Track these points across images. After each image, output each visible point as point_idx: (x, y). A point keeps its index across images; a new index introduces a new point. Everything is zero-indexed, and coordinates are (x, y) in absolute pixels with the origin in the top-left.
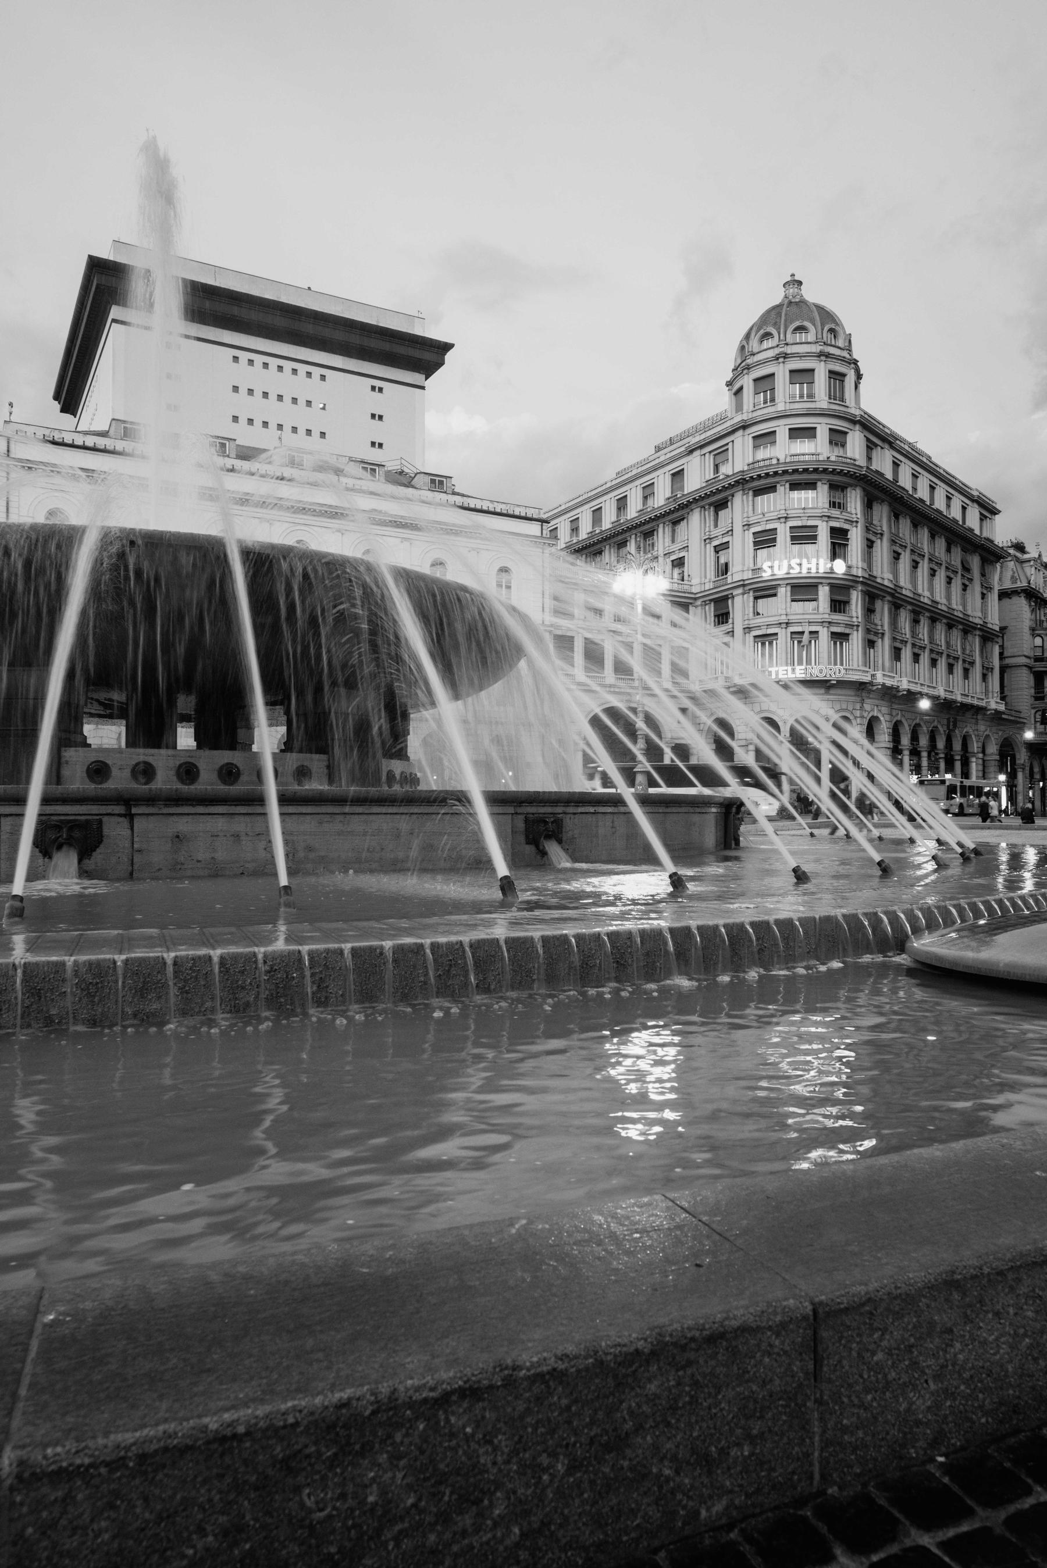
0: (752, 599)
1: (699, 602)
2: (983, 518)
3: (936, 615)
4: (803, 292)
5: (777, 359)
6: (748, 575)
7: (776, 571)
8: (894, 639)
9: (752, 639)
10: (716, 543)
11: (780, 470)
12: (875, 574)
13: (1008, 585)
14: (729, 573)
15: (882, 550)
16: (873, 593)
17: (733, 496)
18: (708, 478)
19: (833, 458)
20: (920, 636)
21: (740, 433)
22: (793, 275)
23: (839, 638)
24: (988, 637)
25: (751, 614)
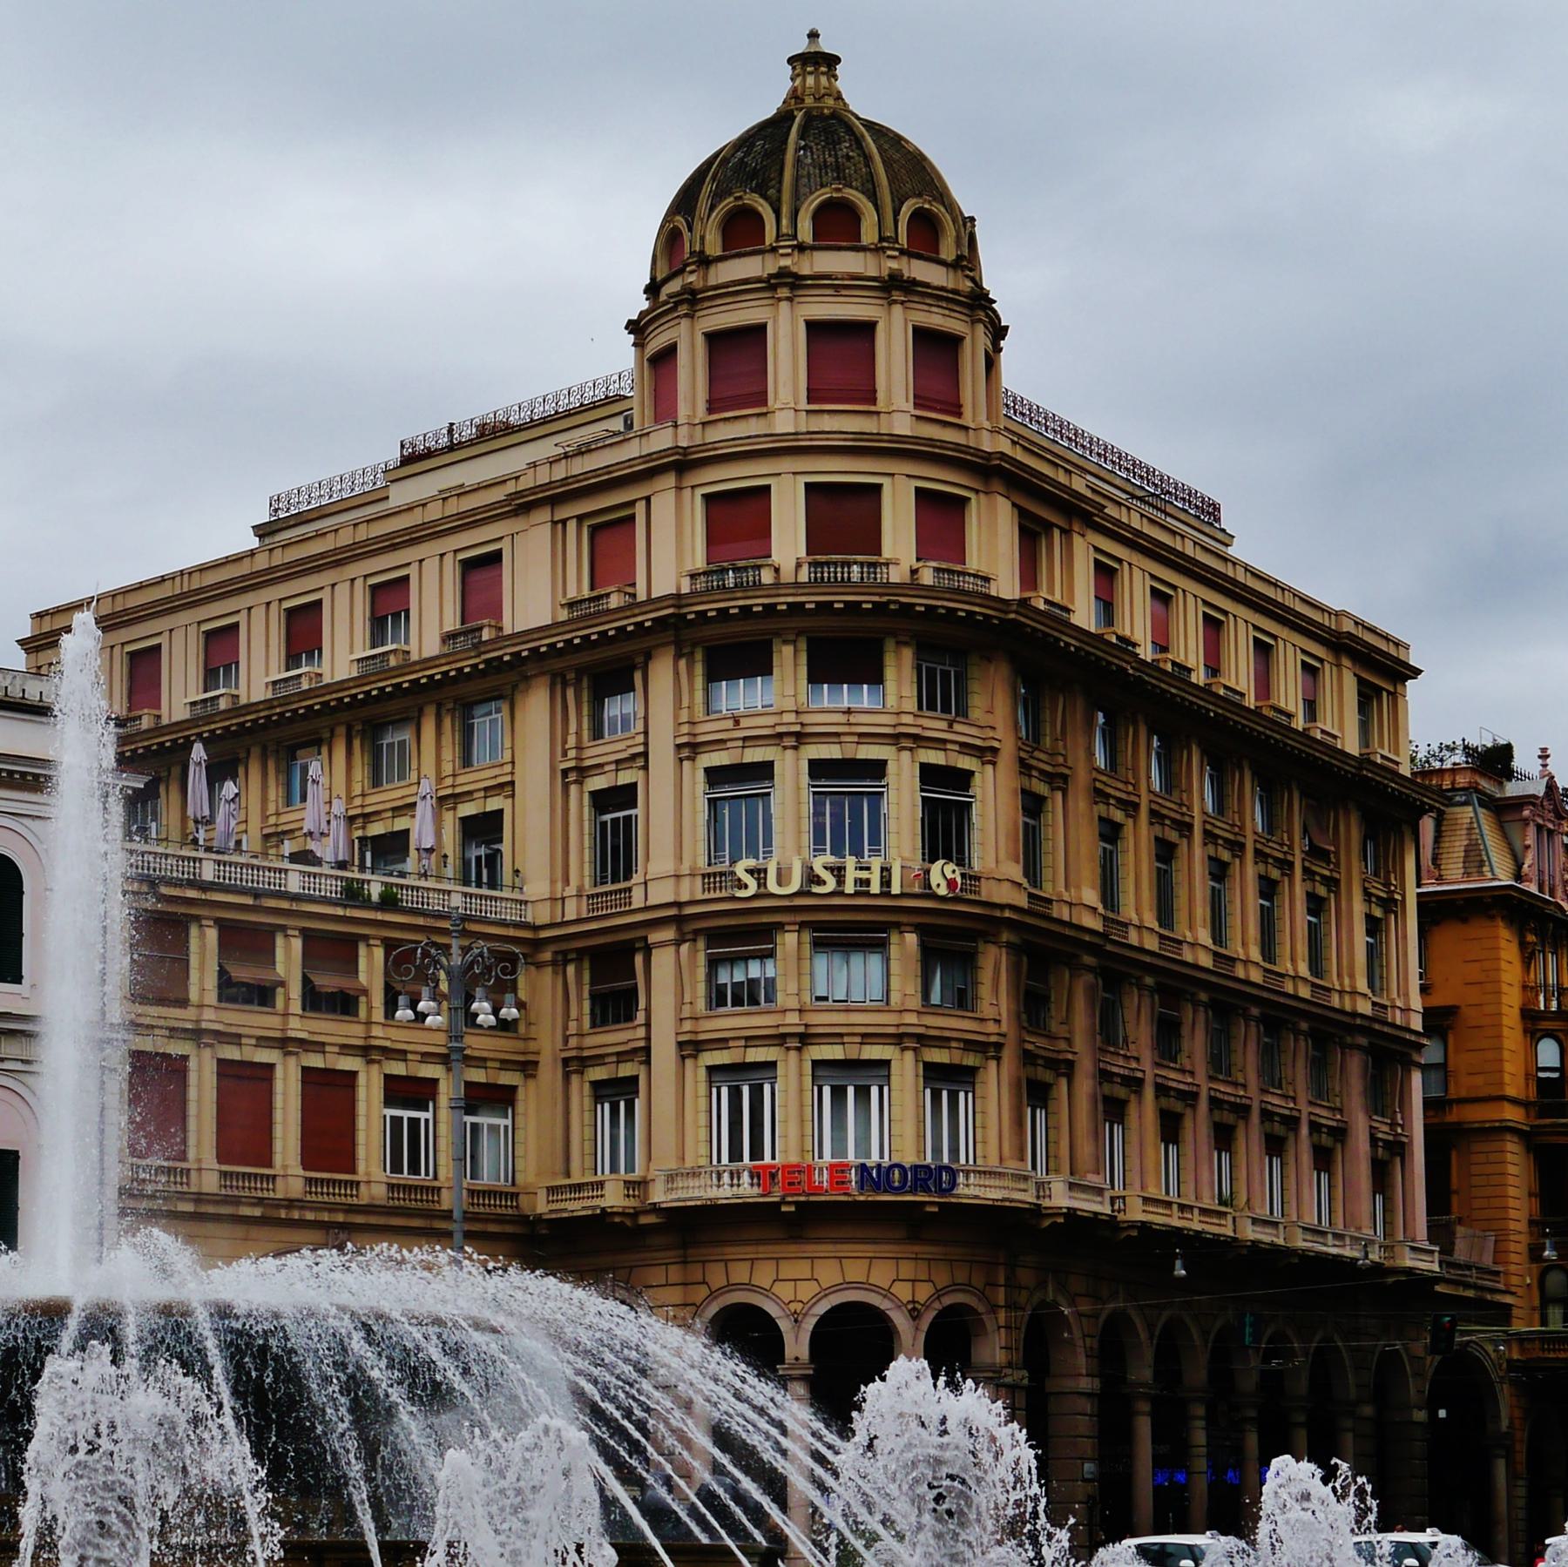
0: (701, 959)
1: (547, 956)
2: (1368, 697)
3: (1227, 1000)
4: (840, 85)
5: (773, 288)
6: (690, 890)
7: (772, 887)
8: (1104, 1076)
9: (702, 1073)
10: (598, 783)
11: (782, 602)
12: (1047, 891)
13: (1456, 879)
14: (637, 878)
15: (1071, 831)
16: (1046, 950)
17: (648, 657)
18: (572, 593)
19: (927, 577)
20: (1184, 1060)
21: (670, 480)
22: (813, 35)
23: (946, 1080)
24: (1387, 1053)
25: (701, 1004)
